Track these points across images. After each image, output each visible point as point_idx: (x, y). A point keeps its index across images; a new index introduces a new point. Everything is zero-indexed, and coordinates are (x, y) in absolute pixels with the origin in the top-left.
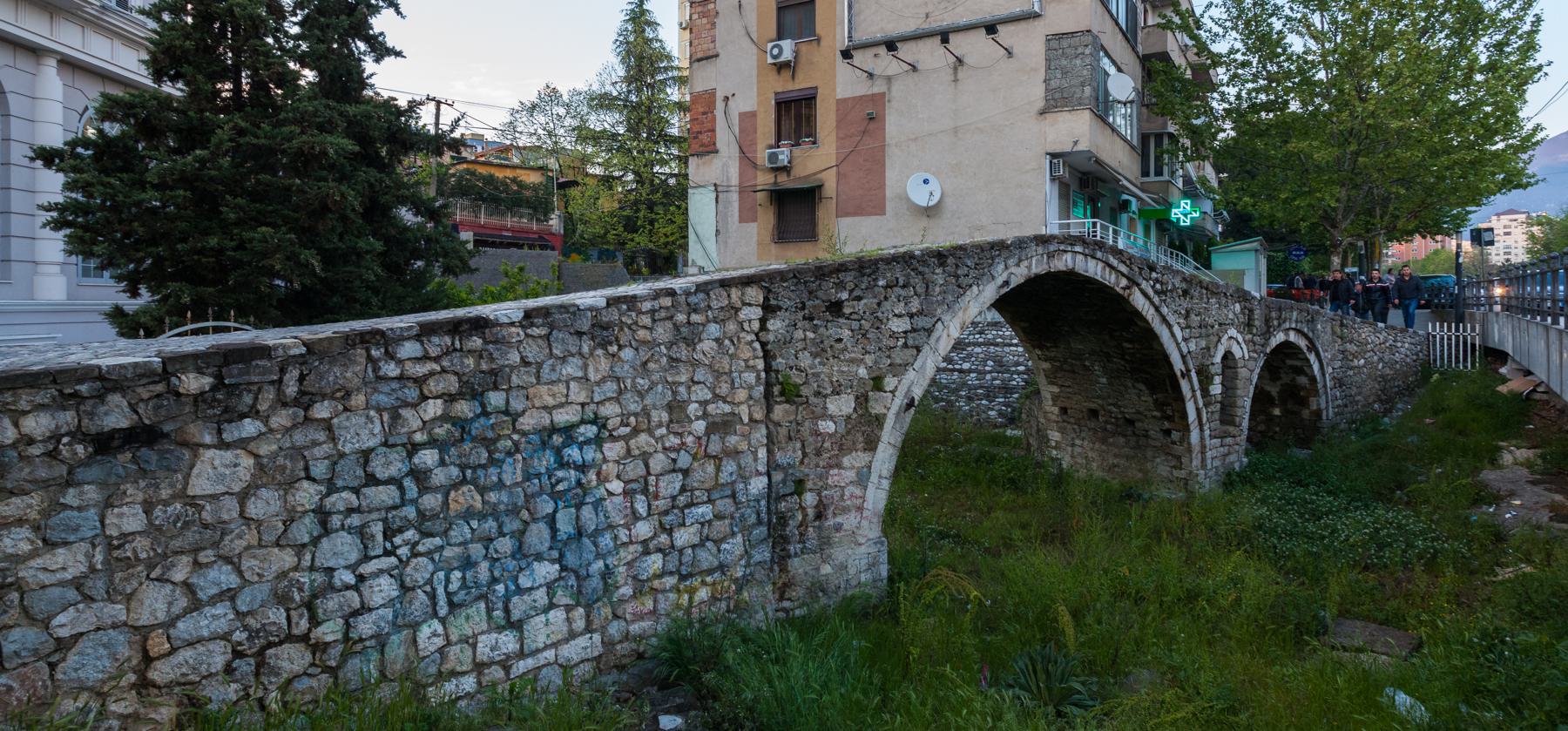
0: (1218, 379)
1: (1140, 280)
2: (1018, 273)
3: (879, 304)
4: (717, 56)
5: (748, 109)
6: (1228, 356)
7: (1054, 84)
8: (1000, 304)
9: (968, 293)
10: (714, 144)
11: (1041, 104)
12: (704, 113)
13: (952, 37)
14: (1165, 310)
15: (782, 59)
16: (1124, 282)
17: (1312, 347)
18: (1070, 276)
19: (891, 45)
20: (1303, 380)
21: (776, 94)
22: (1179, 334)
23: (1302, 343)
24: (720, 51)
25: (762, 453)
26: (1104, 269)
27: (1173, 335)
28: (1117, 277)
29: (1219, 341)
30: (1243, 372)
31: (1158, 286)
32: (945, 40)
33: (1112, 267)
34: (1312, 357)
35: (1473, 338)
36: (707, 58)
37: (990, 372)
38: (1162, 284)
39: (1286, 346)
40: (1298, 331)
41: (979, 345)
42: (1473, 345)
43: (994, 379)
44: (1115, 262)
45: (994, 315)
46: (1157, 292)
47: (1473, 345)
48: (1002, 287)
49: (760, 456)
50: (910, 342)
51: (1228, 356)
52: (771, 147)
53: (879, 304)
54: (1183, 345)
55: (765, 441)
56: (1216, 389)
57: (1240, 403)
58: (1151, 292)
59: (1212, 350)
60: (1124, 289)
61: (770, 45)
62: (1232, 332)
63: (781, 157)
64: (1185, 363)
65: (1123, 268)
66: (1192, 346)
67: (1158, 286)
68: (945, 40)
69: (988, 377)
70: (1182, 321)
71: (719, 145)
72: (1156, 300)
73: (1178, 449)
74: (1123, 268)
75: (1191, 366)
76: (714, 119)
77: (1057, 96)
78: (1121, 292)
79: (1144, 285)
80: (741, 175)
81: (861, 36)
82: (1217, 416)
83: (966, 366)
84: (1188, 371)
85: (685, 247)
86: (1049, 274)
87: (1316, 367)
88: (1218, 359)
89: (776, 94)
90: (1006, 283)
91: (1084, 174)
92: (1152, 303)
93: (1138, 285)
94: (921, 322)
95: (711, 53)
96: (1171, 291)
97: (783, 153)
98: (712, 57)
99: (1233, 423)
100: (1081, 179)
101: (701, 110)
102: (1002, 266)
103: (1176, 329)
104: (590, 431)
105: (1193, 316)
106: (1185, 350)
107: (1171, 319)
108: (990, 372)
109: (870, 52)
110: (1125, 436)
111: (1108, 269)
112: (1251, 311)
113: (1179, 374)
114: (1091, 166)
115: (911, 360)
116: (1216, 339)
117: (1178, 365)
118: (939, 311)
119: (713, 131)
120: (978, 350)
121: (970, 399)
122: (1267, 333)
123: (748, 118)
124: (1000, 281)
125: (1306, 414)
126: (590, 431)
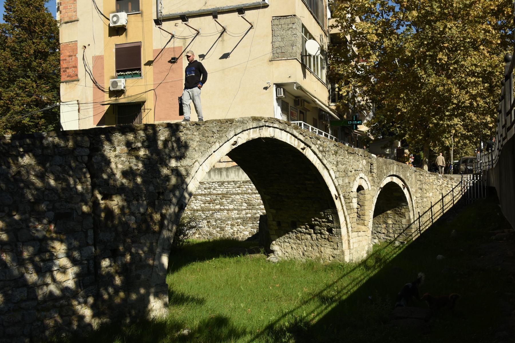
0: (355, 201)
1: (311, 145)
2: (243, 139)
4: (77, 21)
5: (98, 54)
6: (360, 188)
7: (277, 44)
8: (231, 154)
9: (213, 146)
10: (77, 75)
11: (270, 56)
12: (70, 56)
13: (219, 16)
14: (325, 162)
15: (119, 24)
16: (302, 145)
18: (272, 142)
19: (184, 18)
21: (116, 45)
24: (79, 16)
25: (91, 233)
26: (291, 138)
28: (299, 143)
29: (355, 179)
30: (368, 197)
31: (321, 148)
32: (215, 17)
33: (296, 137)
36: (71, 22)
37: (245, 209)
38: (323, 147)
41: (238, 194)
43: (247, 214)
45: (228, 159)
46: (320, 151)
48: (233, 145)
49: (89, 234)
51: (360, 188)
52: (113, 78)
54: (335, 180)
55: (93, 226)
56: (355, 205)
57: (366, 213)
59: (351, 184)
61: (112, 15)
63: (119, 84)
65: (301, 137)
66: (341, 182)
67: (321, 148)
68: (215, 17)
69: (244, 212)
70: (334, 168)
71: (80, 76)
72: (320, 155)
73: (336, 239)
74: (301, 137)
75: (340, 193)
76: (76, 59)
77: (279, 51)
78: (301, 151)
79: (313, 147)
80: (94, 94)
81: (165, 12)
82: (355, 220)
83: (231, 207)
84: (339, 195)
86: (260, 139)
88: (355, 189)
89: (116, 45)
90: (236, 142)
91: (296, 97)
92: (318, 158)
93: (310, 147)
95: (74, 19)
96: (328, 151)
97: (121, 81)
98: (75, 21)
100: (295, 101)
101: (68, 54)
103: (332, 172)
105: (340, 166)
106: (337, 184)
108: (245, 209)
109: (173, 23)
110: (310, 234)
111: (293, 138)
114: (300, 93)
116: (353, 178)
118: (196, 156)
119: (76, 67)
120: (238, 197)
121: (232, 225)
123: (98, 60)
124: (232, 141)
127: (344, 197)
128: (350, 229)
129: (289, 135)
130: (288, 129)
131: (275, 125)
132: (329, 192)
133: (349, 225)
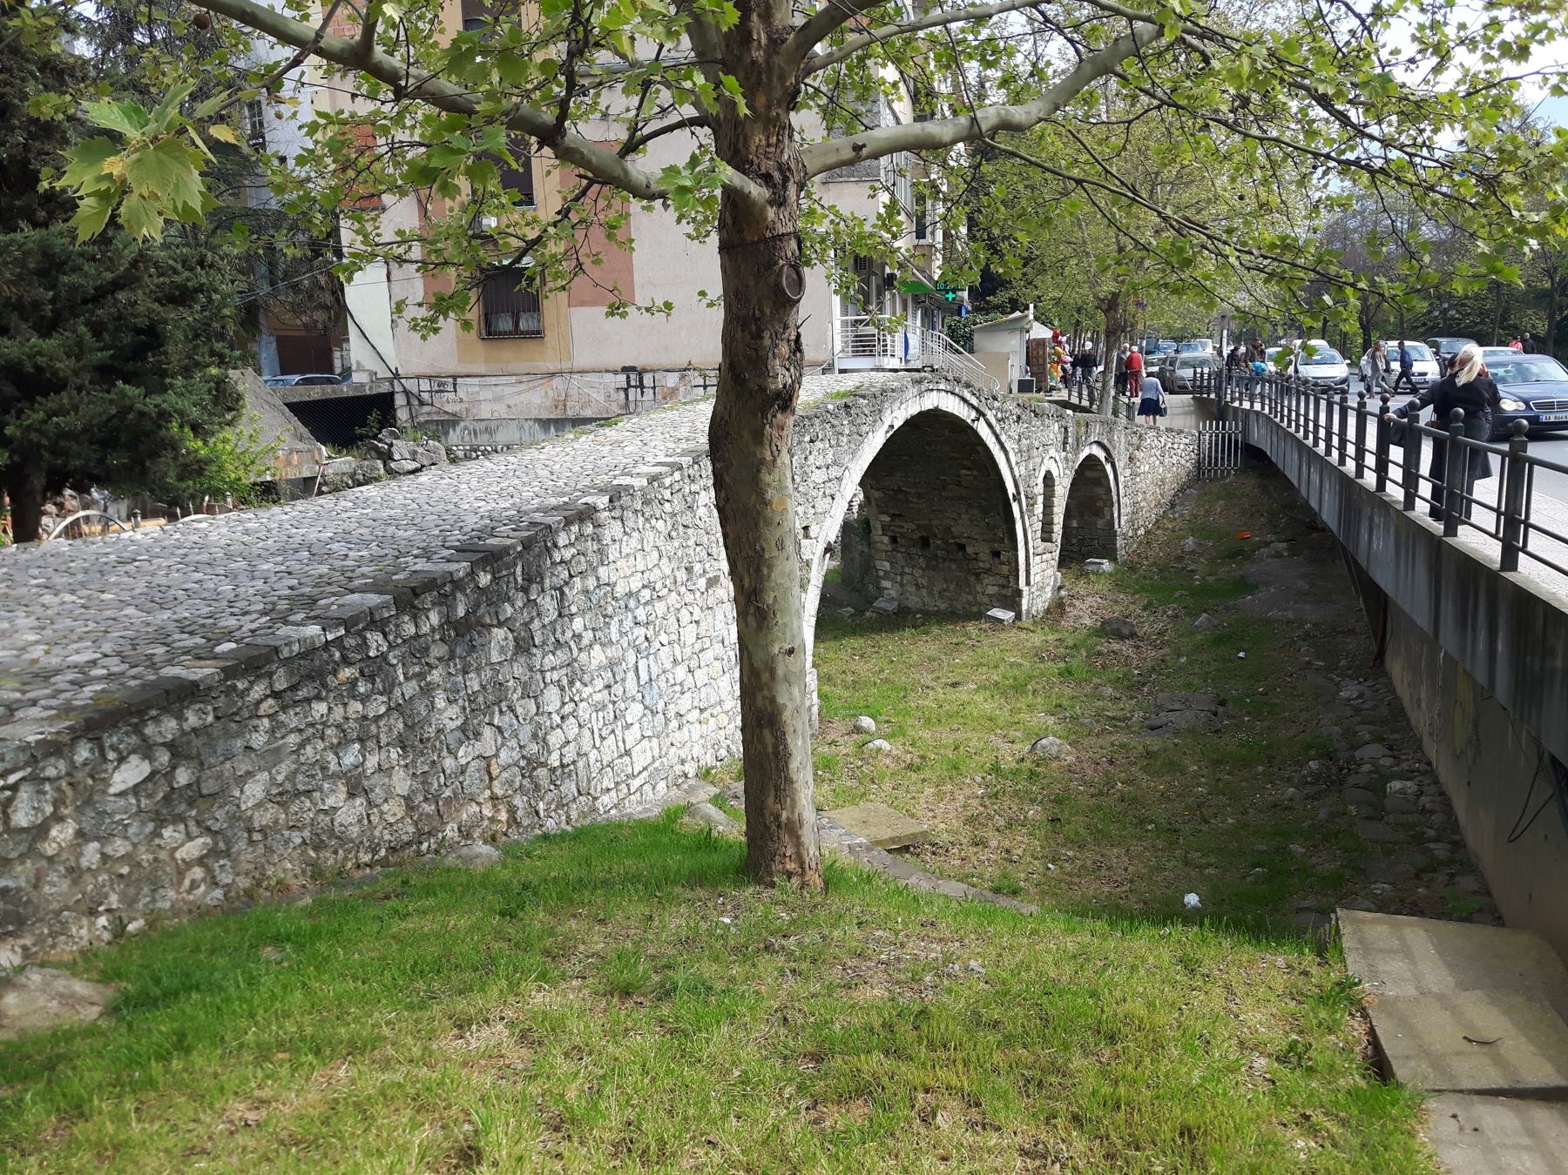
3: (806, 458)
14: (1003, 438)
16: (974, 414)
17: (1109, 458)
20: (1100, 491)
22: (1013, 459)
23: (1101, 455)
27: (1008, 460)
34: (1108, 468)
35: (1236, 435)
39: (1091, 458)
40: (1099, 443)
42: (1236, 441)
44: (967, 395)
46: (999, 421)
47: (1236, 441)
50: (828, 492)
53: (806, 458)
54: (1016, 469)
58: (993, 421)
60: (973, 421)
62: (1052, 452)
64: (1016, 486)
72: (998, 429)
74: (974, 401)
75: (1022, 489)
84: (1019, 493)
85: (343, 338)
86: (921, 413)
87: (1111, 477)
88: (1040, 480)
90: (892, 426)
93: (984, 415)
94: (834, 472)
99: (1050, 541)
102: (889, 411)
104: (646, 594)
106: (1017, 474)
107: (1007, 445)
112: (1066, 429)
113: (1011, 497)
115: (828, 507)
117: (1011, 490)
122: (1077, 450)
125: (1100, 523)
126: (646, 594)
127: (1027, 497)
128: (1031, 551)
129: (957, 399)
130: (957, 391)
131: (942, 387)
132: (1005, 490)
133: (1030, 545)
